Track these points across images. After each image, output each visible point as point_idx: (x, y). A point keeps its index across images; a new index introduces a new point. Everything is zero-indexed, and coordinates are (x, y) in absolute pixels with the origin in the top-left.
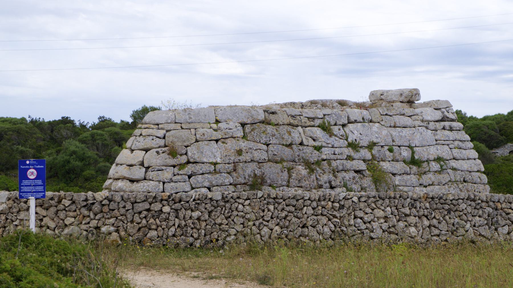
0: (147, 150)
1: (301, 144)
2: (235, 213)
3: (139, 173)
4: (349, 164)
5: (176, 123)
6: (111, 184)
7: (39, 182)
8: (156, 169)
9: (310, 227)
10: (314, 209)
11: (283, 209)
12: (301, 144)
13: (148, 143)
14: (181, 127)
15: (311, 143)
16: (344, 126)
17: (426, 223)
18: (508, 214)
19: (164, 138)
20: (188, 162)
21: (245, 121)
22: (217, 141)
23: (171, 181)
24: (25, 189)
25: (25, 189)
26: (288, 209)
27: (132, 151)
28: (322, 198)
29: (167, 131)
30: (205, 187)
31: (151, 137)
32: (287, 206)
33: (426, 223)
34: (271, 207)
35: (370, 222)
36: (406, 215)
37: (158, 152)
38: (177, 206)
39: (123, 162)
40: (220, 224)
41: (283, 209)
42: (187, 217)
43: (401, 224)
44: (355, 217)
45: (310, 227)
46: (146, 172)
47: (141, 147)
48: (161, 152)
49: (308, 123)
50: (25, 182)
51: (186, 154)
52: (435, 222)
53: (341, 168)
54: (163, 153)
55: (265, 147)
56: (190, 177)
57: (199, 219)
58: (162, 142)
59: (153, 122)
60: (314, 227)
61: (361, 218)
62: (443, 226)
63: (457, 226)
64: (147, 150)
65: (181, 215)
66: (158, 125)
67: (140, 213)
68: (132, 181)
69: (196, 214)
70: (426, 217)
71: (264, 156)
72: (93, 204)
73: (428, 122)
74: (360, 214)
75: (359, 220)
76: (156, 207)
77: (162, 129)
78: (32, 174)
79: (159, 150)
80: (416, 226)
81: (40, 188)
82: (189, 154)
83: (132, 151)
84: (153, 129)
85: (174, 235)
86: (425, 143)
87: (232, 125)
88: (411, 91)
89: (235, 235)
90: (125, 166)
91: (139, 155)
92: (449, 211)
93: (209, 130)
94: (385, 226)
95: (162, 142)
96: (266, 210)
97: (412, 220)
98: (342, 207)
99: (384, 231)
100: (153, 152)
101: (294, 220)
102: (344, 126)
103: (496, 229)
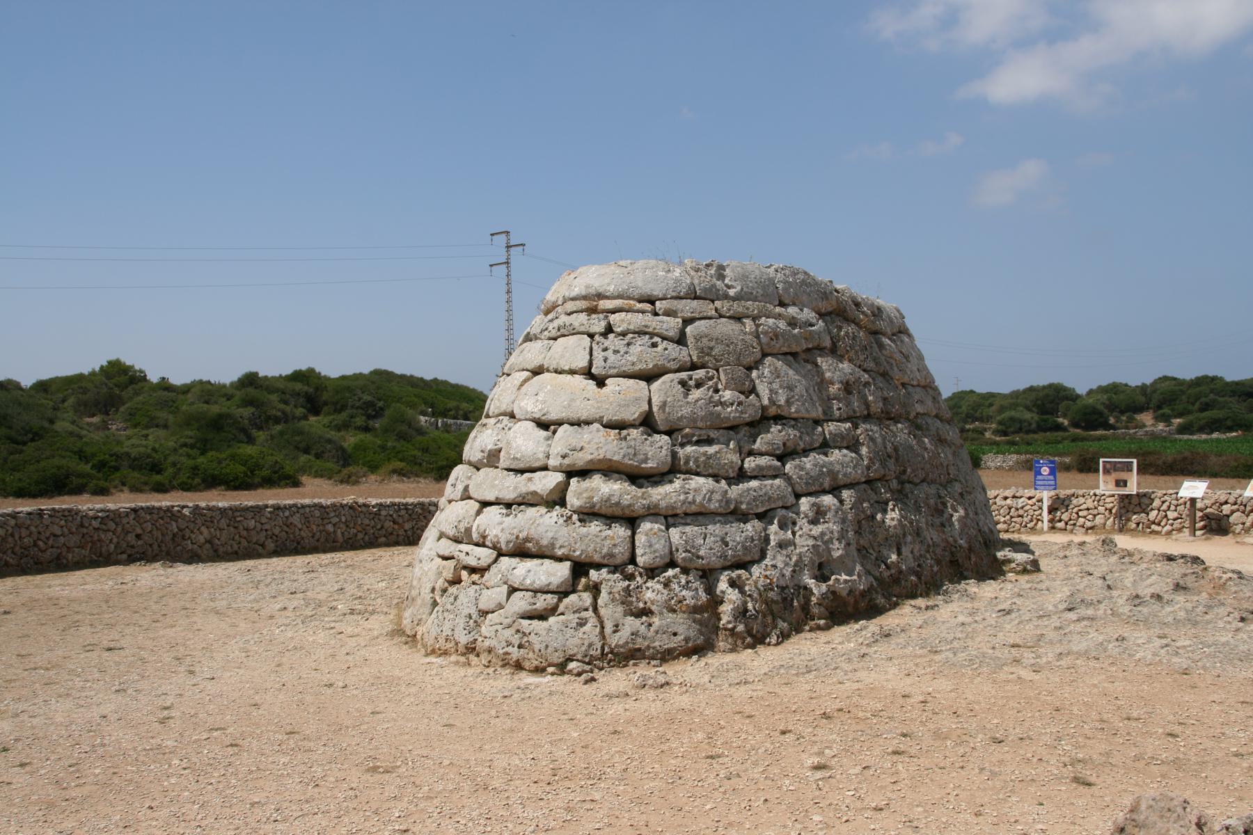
0: (649, 377)
3: (656, 450)
5: (696, 298)
6: (562, 489)
8: (695, 439)
23: (742, 475)
27: (601, 383)
29: (687, 322)
30: (825, 492)
47: (628, 369)
48: (692, 383)
51: (753, 390)
56: (782, 458)
59: (636, 293)
66: (653, 303)
68: (637, 477)
77: (668, 313)
79: (684, 375)
83: (601, 383)
84: (643, 312)
87: (808, 314)
90: (596, 425)
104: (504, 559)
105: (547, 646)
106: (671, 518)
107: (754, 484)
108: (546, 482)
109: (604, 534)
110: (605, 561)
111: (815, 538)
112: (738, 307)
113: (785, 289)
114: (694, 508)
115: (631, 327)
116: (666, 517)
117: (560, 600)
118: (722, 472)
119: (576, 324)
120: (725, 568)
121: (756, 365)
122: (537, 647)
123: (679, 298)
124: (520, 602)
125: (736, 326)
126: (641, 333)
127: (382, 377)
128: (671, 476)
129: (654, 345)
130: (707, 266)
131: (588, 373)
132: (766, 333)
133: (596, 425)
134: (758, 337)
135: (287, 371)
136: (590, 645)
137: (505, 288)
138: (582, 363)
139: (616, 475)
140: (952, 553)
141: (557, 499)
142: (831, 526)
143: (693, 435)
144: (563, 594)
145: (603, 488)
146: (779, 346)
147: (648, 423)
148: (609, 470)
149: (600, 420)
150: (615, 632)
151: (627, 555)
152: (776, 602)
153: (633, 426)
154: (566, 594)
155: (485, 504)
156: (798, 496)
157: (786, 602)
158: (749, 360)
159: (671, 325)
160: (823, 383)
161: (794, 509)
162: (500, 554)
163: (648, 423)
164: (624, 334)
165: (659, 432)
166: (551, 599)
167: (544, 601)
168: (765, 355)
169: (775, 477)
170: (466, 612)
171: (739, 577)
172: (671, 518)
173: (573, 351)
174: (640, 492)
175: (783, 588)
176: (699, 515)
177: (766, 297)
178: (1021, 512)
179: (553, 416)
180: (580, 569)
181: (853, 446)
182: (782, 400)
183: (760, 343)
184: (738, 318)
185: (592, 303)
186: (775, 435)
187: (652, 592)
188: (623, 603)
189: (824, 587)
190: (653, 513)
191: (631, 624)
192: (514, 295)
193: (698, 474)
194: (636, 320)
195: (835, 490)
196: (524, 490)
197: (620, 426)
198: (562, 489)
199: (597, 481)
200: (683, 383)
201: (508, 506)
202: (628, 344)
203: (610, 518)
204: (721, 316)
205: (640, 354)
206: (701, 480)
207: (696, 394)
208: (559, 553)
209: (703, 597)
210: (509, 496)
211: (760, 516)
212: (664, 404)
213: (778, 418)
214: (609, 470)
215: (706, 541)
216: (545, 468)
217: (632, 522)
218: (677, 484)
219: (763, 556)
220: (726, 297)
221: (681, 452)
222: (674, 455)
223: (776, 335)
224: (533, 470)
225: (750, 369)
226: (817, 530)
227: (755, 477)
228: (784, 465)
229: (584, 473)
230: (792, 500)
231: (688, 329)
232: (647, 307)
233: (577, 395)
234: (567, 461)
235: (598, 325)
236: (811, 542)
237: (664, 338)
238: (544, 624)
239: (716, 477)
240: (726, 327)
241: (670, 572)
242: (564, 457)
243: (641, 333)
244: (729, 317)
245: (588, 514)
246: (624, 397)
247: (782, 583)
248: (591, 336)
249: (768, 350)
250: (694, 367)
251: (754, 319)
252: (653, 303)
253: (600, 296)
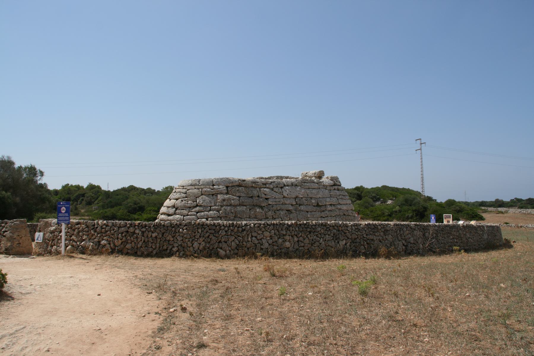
0: (177, 199)
1: (258, 196)
2: (177, 234)
3: (172, 211)
4: (283, 207)
7: (67, 214)
9: (223, 243)
10: (226, 231)
11: (207, 232)
12: (258, 196)
13: (178, 196)
15: (263, 196)
16: (282, 188)
17: (296, 239)
18: (345, 233)
20: (197, 206)
21: (228, 185)
22: (213, 195)
23: (188, 215)
24: (60, 218)
25: (60, 218)
26: (210, 231)
28: (231, 225)
32: (209, 229)
33: (296, 239)
34: (200, 231)
35: (261, 239)
36: (284, 235)
37: (182, 201)
38: (144, 229)
40: (169, 241)
41: (207, 232)
42: (149, 236)
43: (280, 240)
44: (252, 236)
45: (223, 243)
49: (262, 186)
50: (60, 215)
52: (301, 239)
53: (279, 208)
55: (238, 198)
56: (197, 213)
57: (156, 237)
58: (185, 195)
60: (226, 242)
61: (256, 237)
62: (307, 241)
63: (314, 241)
64: (177, 199)
65: (145, 235)
67: (122, 233)
68: (169, 215)
69: (154, 235)
70: (296, 235)
71: (237, 202)
72: (97, 227)
73: (327, 186)
74: (254, 234)
75: (254, 238)
76: (131, 230)
78: (63, 210)
80: (289, 241)
81: (67, 218)
82: (198, 201)
85: (141, 247)
86: (324, 196)
88: (320, 172)
89: (177, 247)
91: (173, 201)
92: (310, 232)
93: (208, 190)
94: (270, 242)
95: (185, 195)
96: (197, 232)
97: (287, 237)
98: (243, 230)
99: (269, 245)
100: (180, 200)
101: (213, 238)
102: (282, 188)
103: (338, 242)
112: (199, 187)
113: (216, 183)
125: (197, 190)
127: (385, 187)
135: (354, 187)
137: (420, 158)
159: (184, 191)
160: (217, 199)
163: (174, 207)
168: (202, 195)
177: (207, 185)
181: (218, 211)
184: (198, 189)
186: (198, 209)
192: (423, 160)
197: (168, 207)
213: (201, 206)
220: (198, 185)
229: (162, 214)
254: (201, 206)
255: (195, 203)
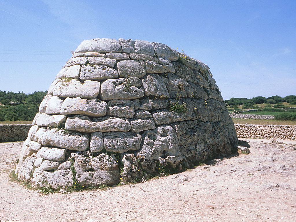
0: (101, 81)
6: (64, 121)
8: (117, 104)
14: (130, 57)
19: (115, 67)
23: (135, 118)
29: (118, 61)
30: (168, 125)
31: (101, 66)
39: (74, 94)
46: (108, 106)
51: (142, 87)
54: (120, 84)
66: (105, 54)
68: (92, 118)
79: (114, 80)
82: (145, 86)
83: (82, 82)
90: (79, 98)
104: (43, 148)
105: (52, 183)
106: (104, 134)
107: (140, 120)
108: (58, 119)
109: (77, 139)
110: (78, 149)
111: (162, 141)
112: (137, 56)
114: (114, 130)
115: (96, 62)
116: (103, 133)
117: (59, 165)
118: (127, 116)
119: (76, 61)
120: (125, 153)
121: (145, 77)
122: (49, 183)
123: (115, 52)
124: (45, 165)
126: (99, 64)
128: (106, 118)
129: (104, 69)
130: (128, 41)
131: (79, 79)
132: (148, 66)
133: (79, 98)
134: (145, 67)
136: (69, 182)
138: (76, 74)
139: (84, 117)
140: (217, 147)
141: (61, 125)
142: (169, 137)
143: (116, 102)
144: (61, 161)
145: (79, 122)
146: (154, 71)
147: (99, 98)
148: (81, 115)
149: (80, 96)
150: (79, 177)
151: (86, 147)
152: (144, 166)
153: (93, 98)
154: (62, 162)
155: (40, 127)
156: (157, 126)
157: (149, 167)
158: (140, 76)
161: (155, 131)
162: (42, 146)
163: (99, 98)
164: (93, 65)
165: (103, 101)
166: (56, 164)
167: (54, 164)
169: (148, 118)
170: (29, 167)
171: (130, 156)
172: (104, 134)
173: (74, 71)
174: (92, 123)
175: (148, 161)
176: (115, 133)
178: (247, 131)
179: (63, 94)
180: (68, 153)
182: (153, 89)
183: (146, 69)
184: (138, 60)
185: (83, 53)
186: (150, 103)
187: (95, 162)
188: (83, 166)
189: (164, 160)
190: (97, 131)
191: (86, 174)
193: (117, 117)
194: (97, 60)
195: (172, 124)
196: (51, 121)
197: (87, 98)
198: (64, 121)
199: (77, 119)
200: (114, 83)
201: (46, 127)
202: (94, 68)
203: (81, 134)
204: (131, 59)
205: (98, 71)
206: (118, 119)
207: (119, 87)
208: (61, 146)
209: (115, 163)
210: (46, 124)
211: (141, 133)
212: (105, 91)
214: (81, 115)
215: (117, 143)
216: (59, 114)
217: (89, 135)
218: (107, 121)
219: (141, 148)
221: (110, 108)
222: (108, 109)
223: (152, 66)
224: (55, 114)
225: (141, 79)
226: (163, 139)
227: (140, 118)
228: (152, 114)
229: (72, 116)
230: (154, 127)
231: (118, 63)
232: (104, 55)
233: (75, 87)
234: (66, 111)
235: (84, 61)
236: (160, 143)
237: (108, 66)
238: (52, 173)
239: (124, 118)
240: (132, 63)
241: (103, 154)
242: (65, 109)
243: (99, 64)
244: (135, 60)
245: (72, 132)
246: (91, 88)
247: (147, 159)
248: (81, 65)
249: (148, 72)
250: (119, 77)
251: (144, 61)
252: (105, 54)
253: (87, 51)
254: (151, 97)
255: (141, 90)
